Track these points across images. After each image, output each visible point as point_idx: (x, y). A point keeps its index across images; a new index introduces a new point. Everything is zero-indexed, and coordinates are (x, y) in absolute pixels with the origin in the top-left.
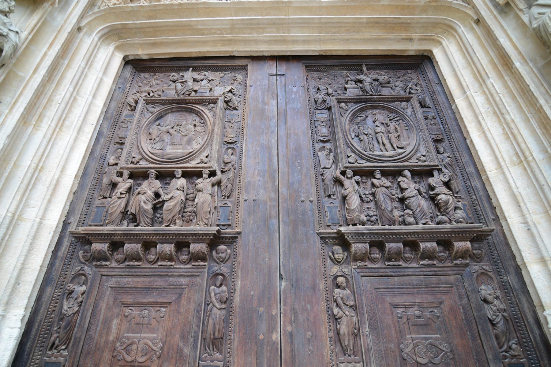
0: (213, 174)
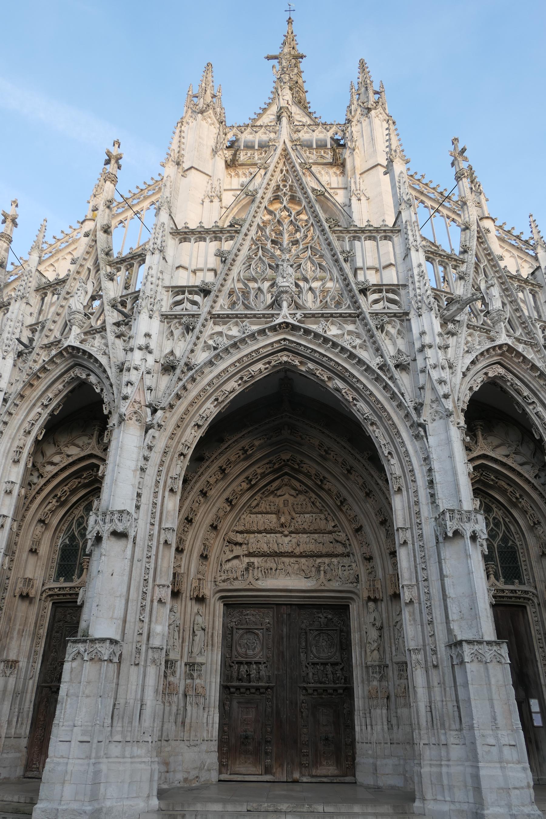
0: (264, 663)
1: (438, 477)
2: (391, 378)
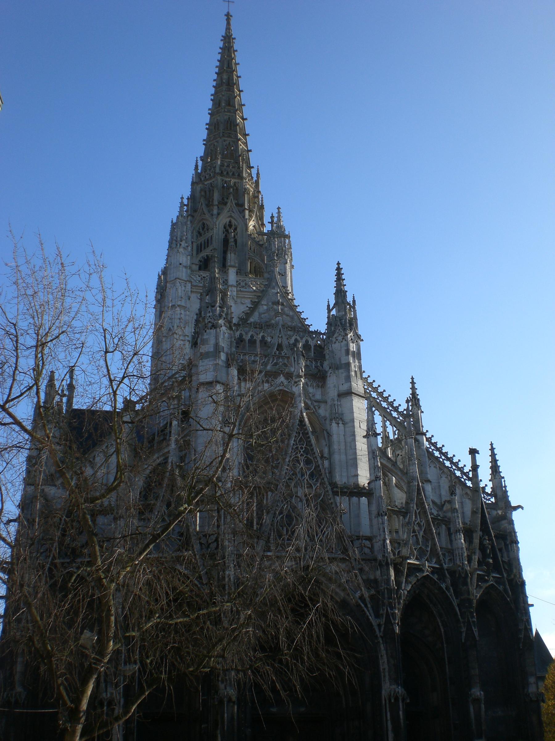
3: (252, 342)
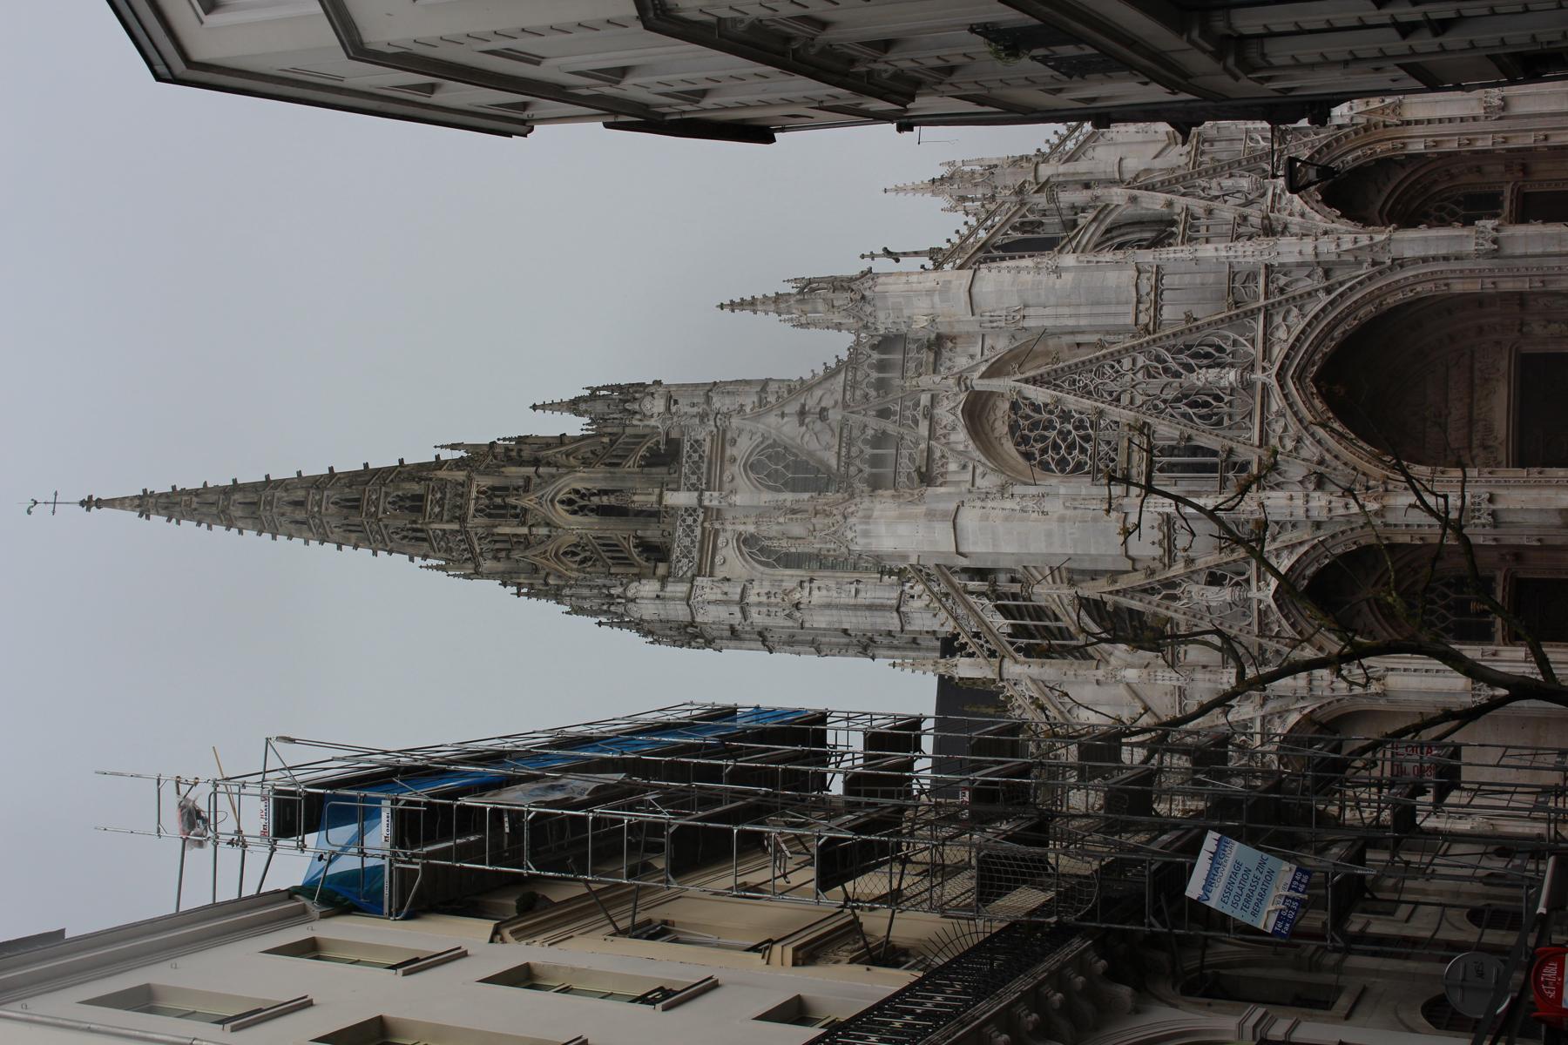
1: (1443, 252)
2: (1341, 284)
3: (876, 461)
